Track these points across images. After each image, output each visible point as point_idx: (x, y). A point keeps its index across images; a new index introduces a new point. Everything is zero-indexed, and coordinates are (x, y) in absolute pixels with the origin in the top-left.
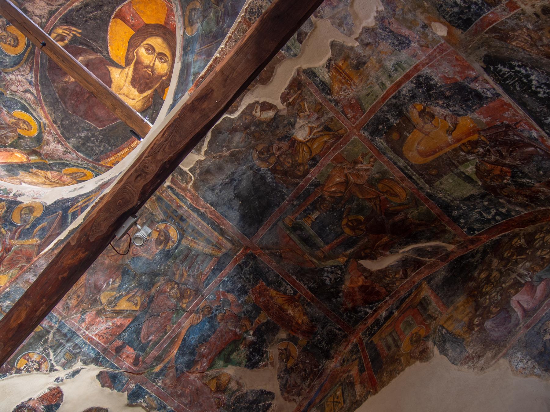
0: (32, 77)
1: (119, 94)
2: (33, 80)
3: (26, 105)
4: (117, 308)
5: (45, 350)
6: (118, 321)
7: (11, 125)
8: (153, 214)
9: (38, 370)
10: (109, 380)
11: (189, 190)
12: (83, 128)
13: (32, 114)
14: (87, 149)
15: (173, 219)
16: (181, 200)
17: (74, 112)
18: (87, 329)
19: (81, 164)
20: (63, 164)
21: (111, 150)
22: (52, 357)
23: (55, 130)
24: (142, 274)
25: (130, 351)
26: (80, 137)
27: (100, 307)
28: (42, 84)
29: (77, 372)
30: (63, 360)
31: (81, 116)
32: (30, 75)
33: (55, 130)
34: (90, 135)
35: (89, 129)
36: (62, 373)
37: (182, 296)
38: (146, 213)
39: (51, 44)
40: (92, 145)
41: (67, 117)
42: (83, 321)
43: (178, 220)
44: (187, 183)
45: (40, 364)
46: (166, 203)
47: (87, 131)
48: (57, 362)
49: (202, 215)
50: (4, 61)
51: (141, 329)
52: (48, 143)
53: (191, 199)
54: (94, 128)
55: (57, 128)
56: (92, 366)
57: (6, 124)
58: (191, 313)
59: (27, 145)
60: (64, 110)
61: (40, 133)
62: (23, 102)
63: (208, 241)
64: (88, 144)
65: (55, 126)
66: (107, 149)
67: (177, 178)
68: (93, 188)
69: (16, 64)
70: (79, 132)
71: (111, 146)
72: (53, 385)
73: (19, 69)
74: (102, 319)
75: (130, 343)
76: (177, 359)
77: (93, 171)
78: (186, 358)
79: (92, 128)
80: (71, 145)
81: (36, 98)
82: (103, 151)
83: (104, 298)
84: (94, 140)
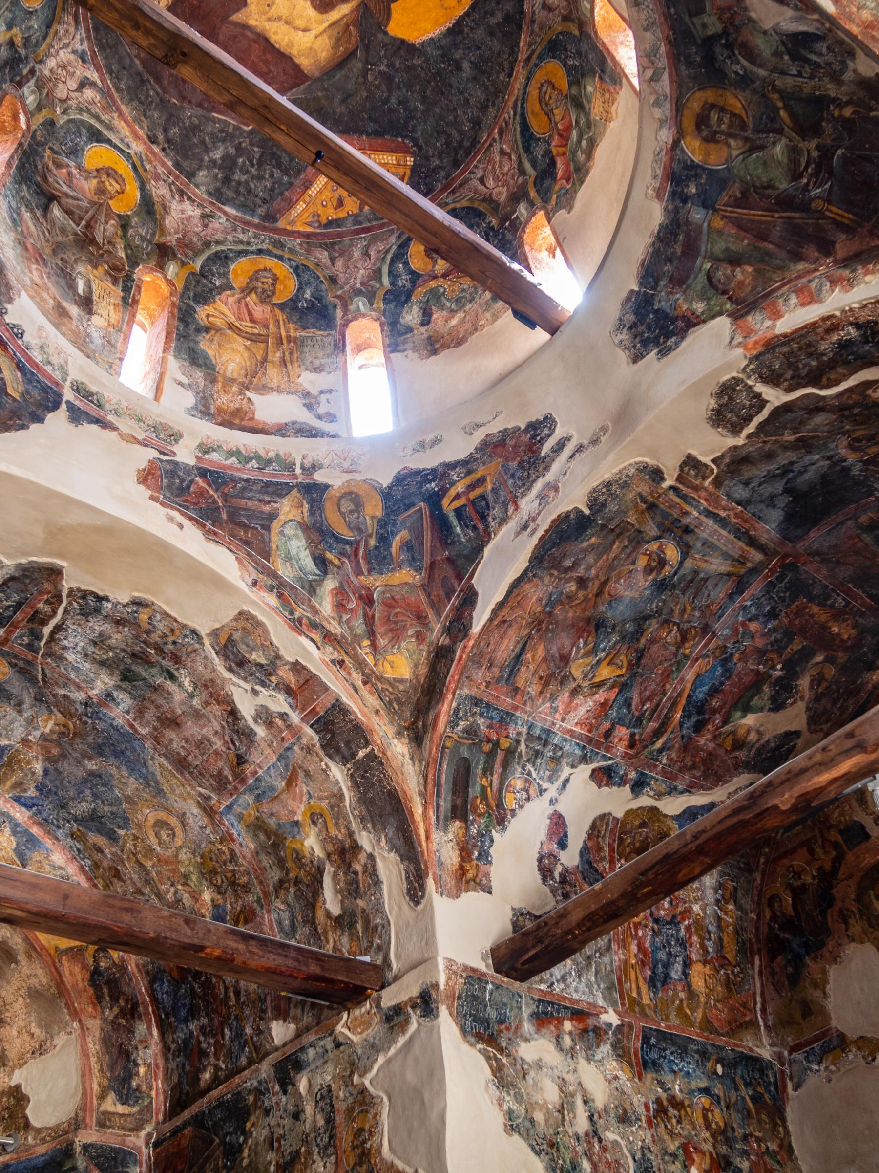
0: (81, 40)
1: (269, 19)
2: (85, 46)
3: (93, 121)
4: (596, 680)
5: (523, 767)
6: (601, 696)
7: (95, 199)
8: (640, 532)
9: (528, 799)
10: (605, 776)
11: (705, 489)
12: (212, 135)
13: (109, 142)
14: (237, 192)
15: (672, 532)
16: (690, 504)
17: (182, 98)
18: (563, 720)
19: (248, 243)
20: (217, 254)
21: (291, 184)
22: (534, 775)
23: (164, 165)
24: (624, 622)
25: (622, 732)
26: (214, 162)
27: (574, 685)
28: (102, 48)
29: (567, 781)
30: (548, 773)
31: (200, 105)
32: (78, 37)
33: (161, 163)
34: (232, 151)
35: (226, 137)
36: (552, 790)
37: (684, 637)
38: (628, 530)
39: (337, 153)
40: (244, 178)
41: (172, 118)
42: (556, 710)
43: (680, 533)
44: (704, 478)
45: (527, 791)
46: (662, 511)
47: (223, 140)
48: (541, 778)
49: (723, 522)
50: (32, 32)
51: (631, 698)
52: (166, 209)
53: (706, 500)
54: (237, 128)
55: (161, 154)
56: (582, 767)
57: (93, 203)
58: (697, 660)
59: (143, 239)
60: (161, 100)
61: (143, 188)
62: (85, 117)
63: (726, 556)
64: (236, 177)
65: (156, 149)
66: (279, 182)
67: (688, 474)
68: (472, 450)
69: (49, 27)
70: (207, 151)
71: (285, 172)
72: (550, 810)
73: (56, 32)
74: (579, 699)
75: (620, 721)
76: (681, 724)
77: (281, 258)
78: (694, 719)
79: (231, 130)
80: (203, 188)
81: (101, 91)
82: (272, 190)
83: (577, 669)
84: (244, 162)
